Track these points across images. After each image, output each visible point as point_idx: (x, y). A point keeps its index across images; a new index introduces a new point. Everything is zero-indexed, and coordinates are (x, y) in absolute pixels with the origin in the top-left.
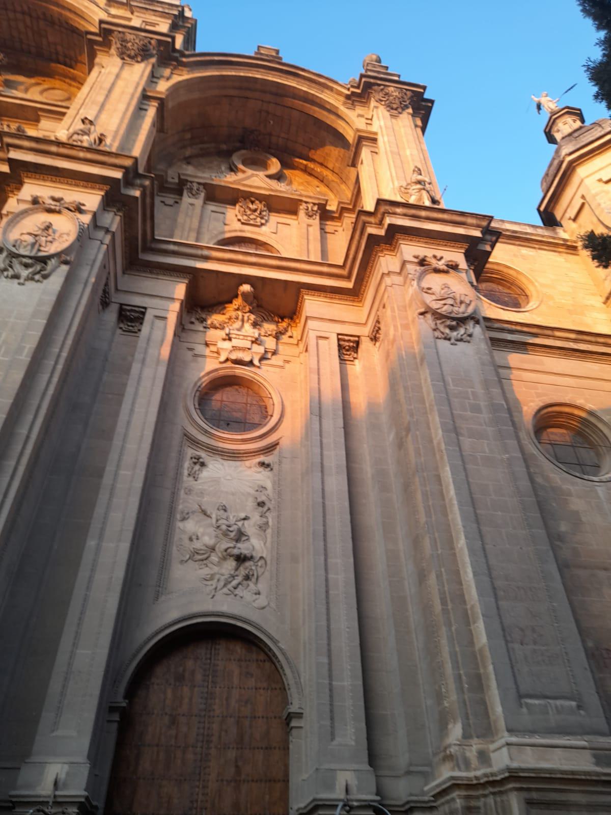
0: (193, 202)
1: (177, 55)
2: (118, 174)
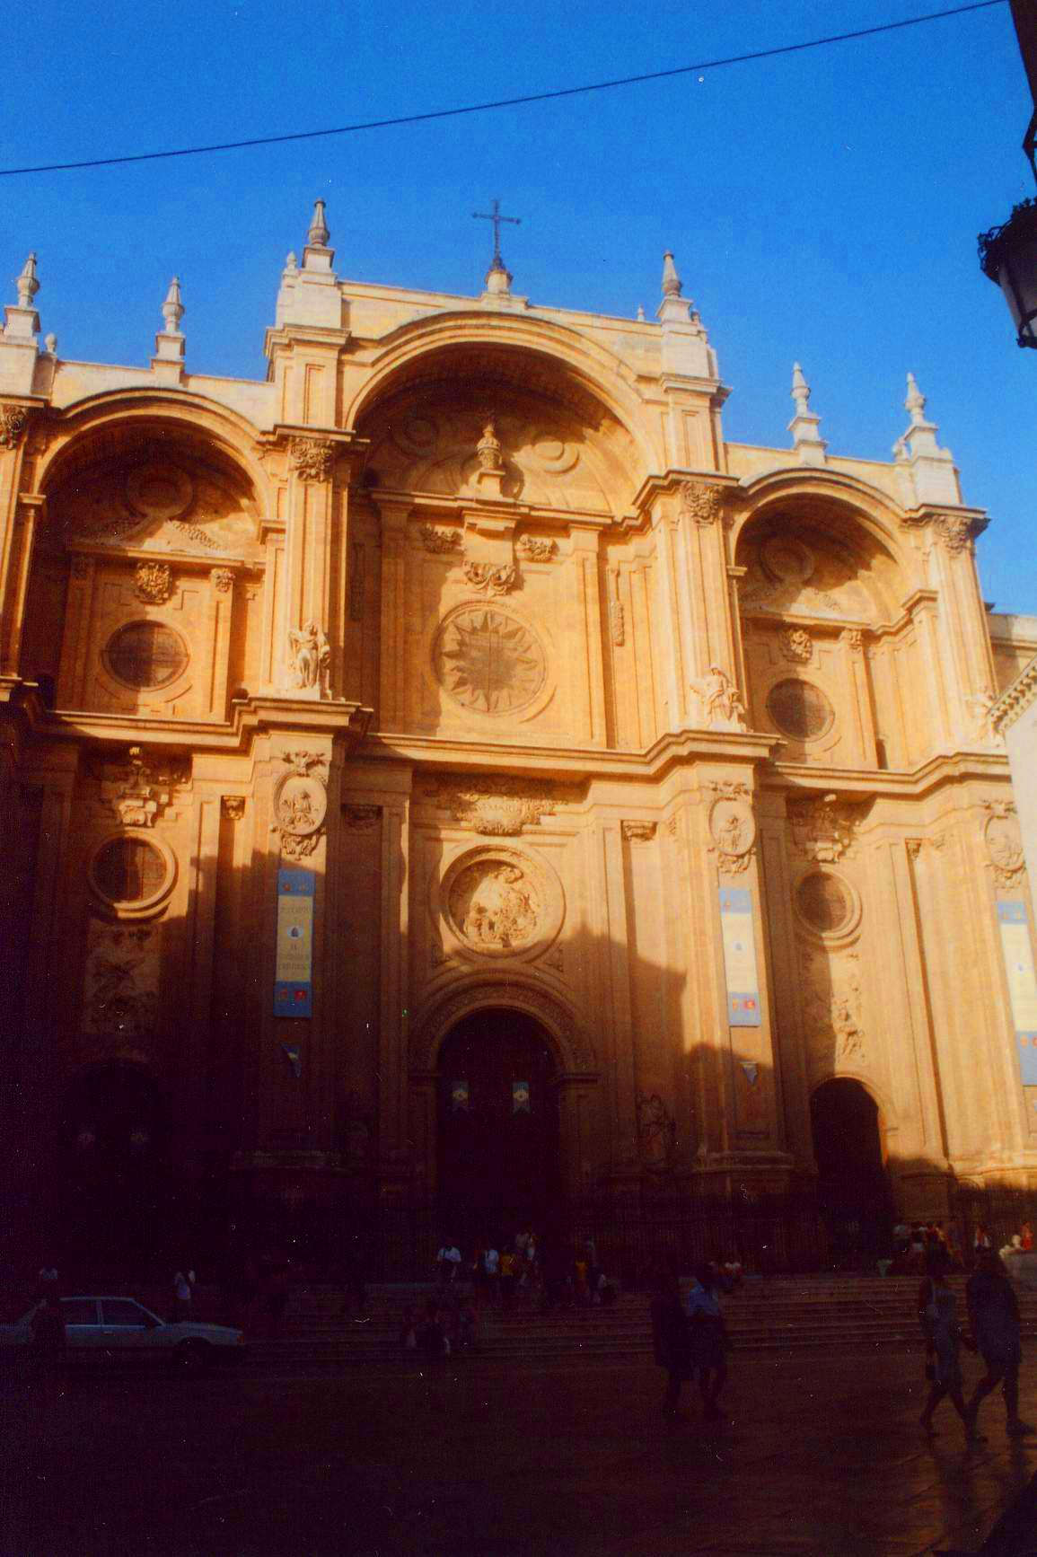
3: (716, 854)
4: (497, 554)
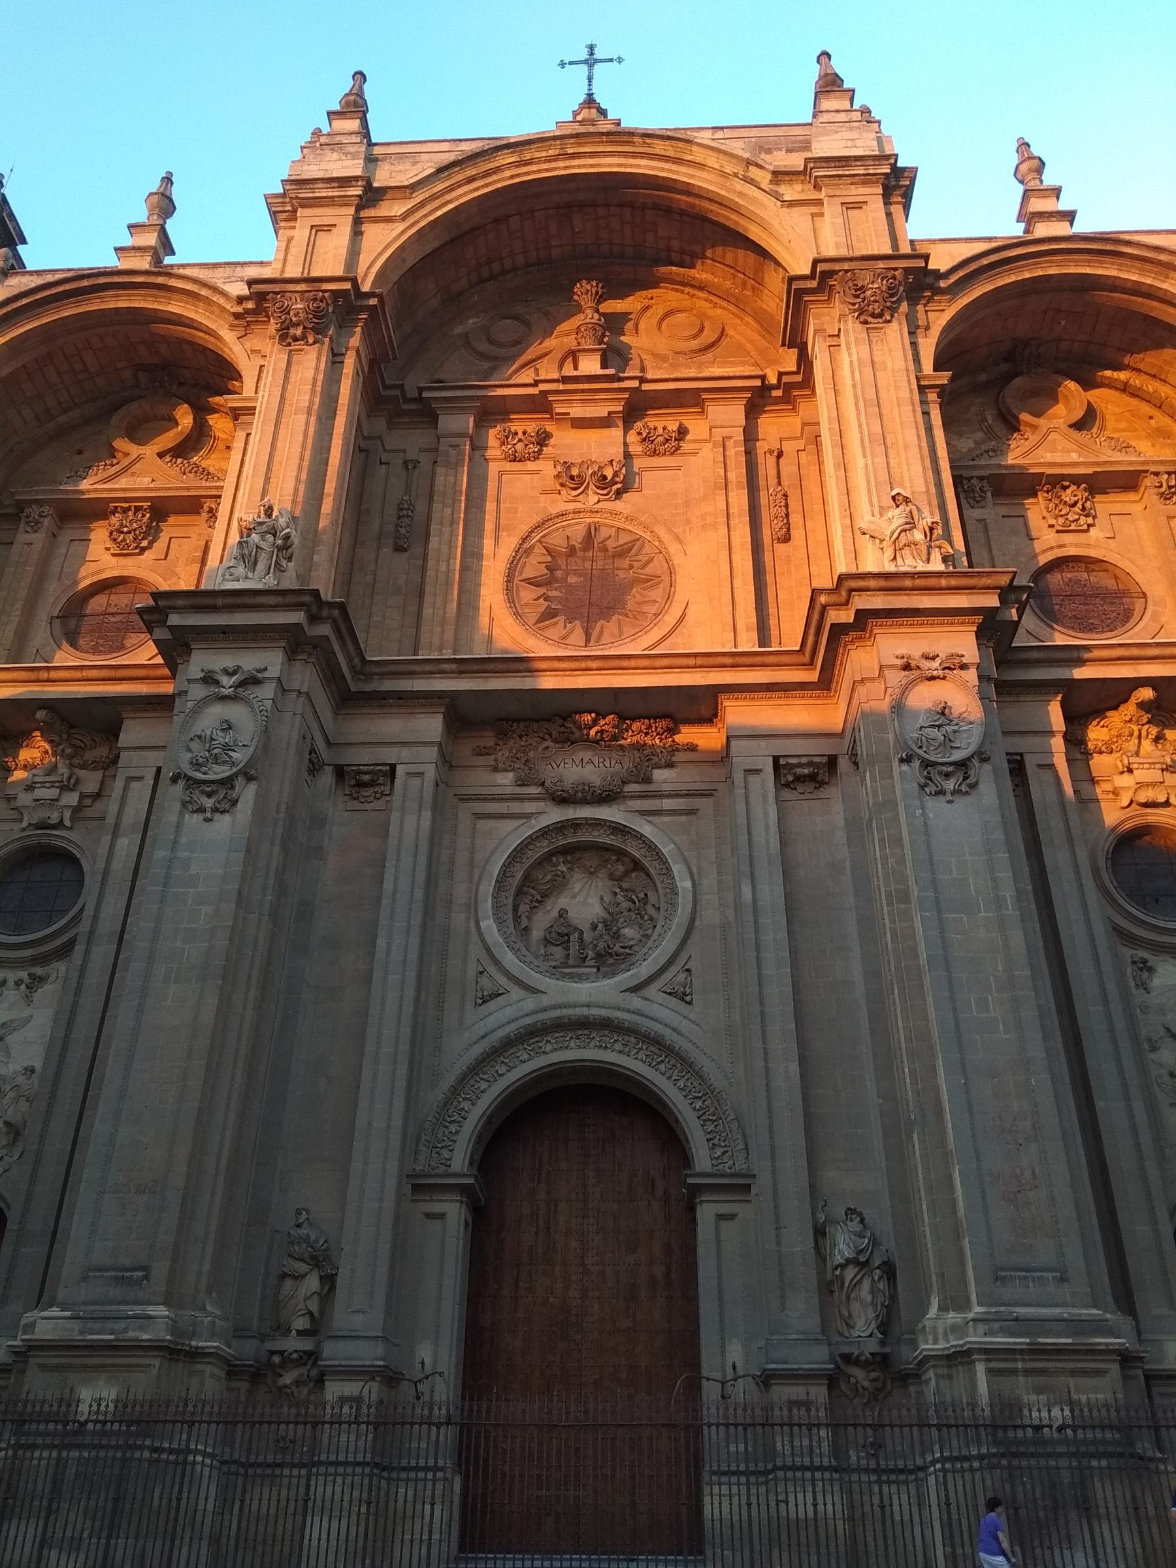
0: (981, 517)
1: (929, 280)
2: (993, 601)
3: (916, 764)
4: (603, 447)
